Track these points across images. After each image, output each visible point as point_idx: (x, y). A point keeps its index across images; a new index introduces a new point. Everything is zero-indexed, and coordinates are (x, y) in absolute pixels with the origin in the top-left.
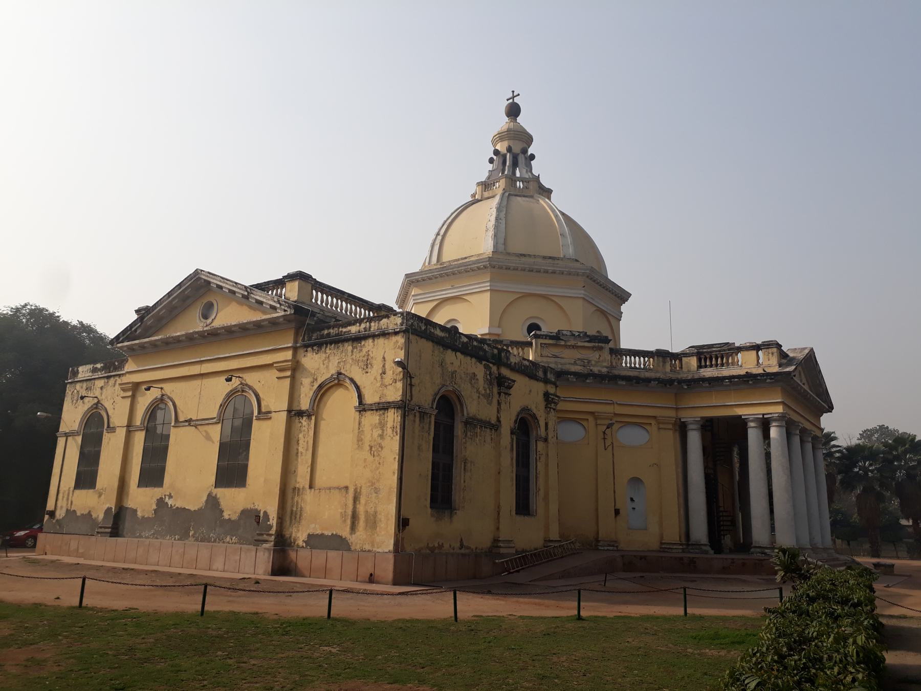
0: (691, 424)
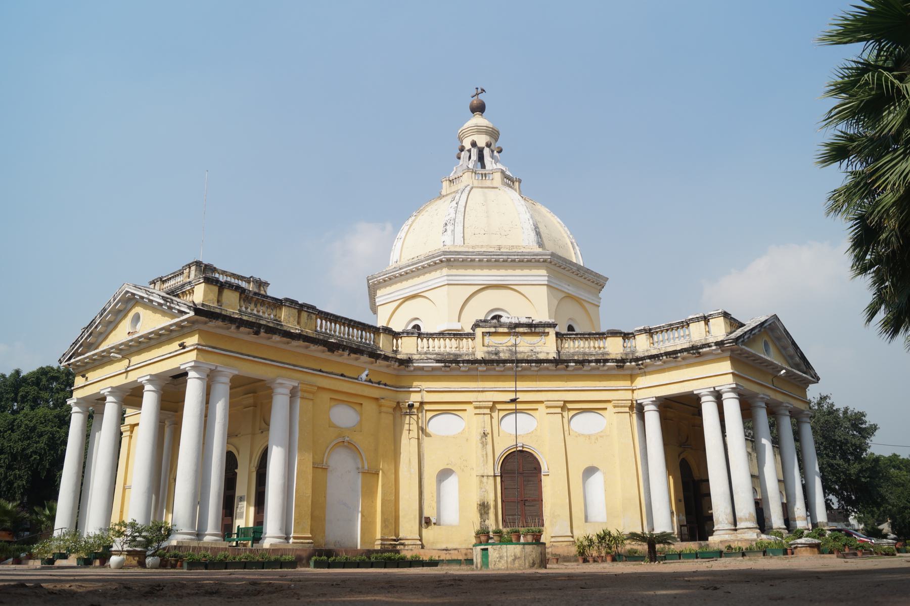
0: (647, 405)
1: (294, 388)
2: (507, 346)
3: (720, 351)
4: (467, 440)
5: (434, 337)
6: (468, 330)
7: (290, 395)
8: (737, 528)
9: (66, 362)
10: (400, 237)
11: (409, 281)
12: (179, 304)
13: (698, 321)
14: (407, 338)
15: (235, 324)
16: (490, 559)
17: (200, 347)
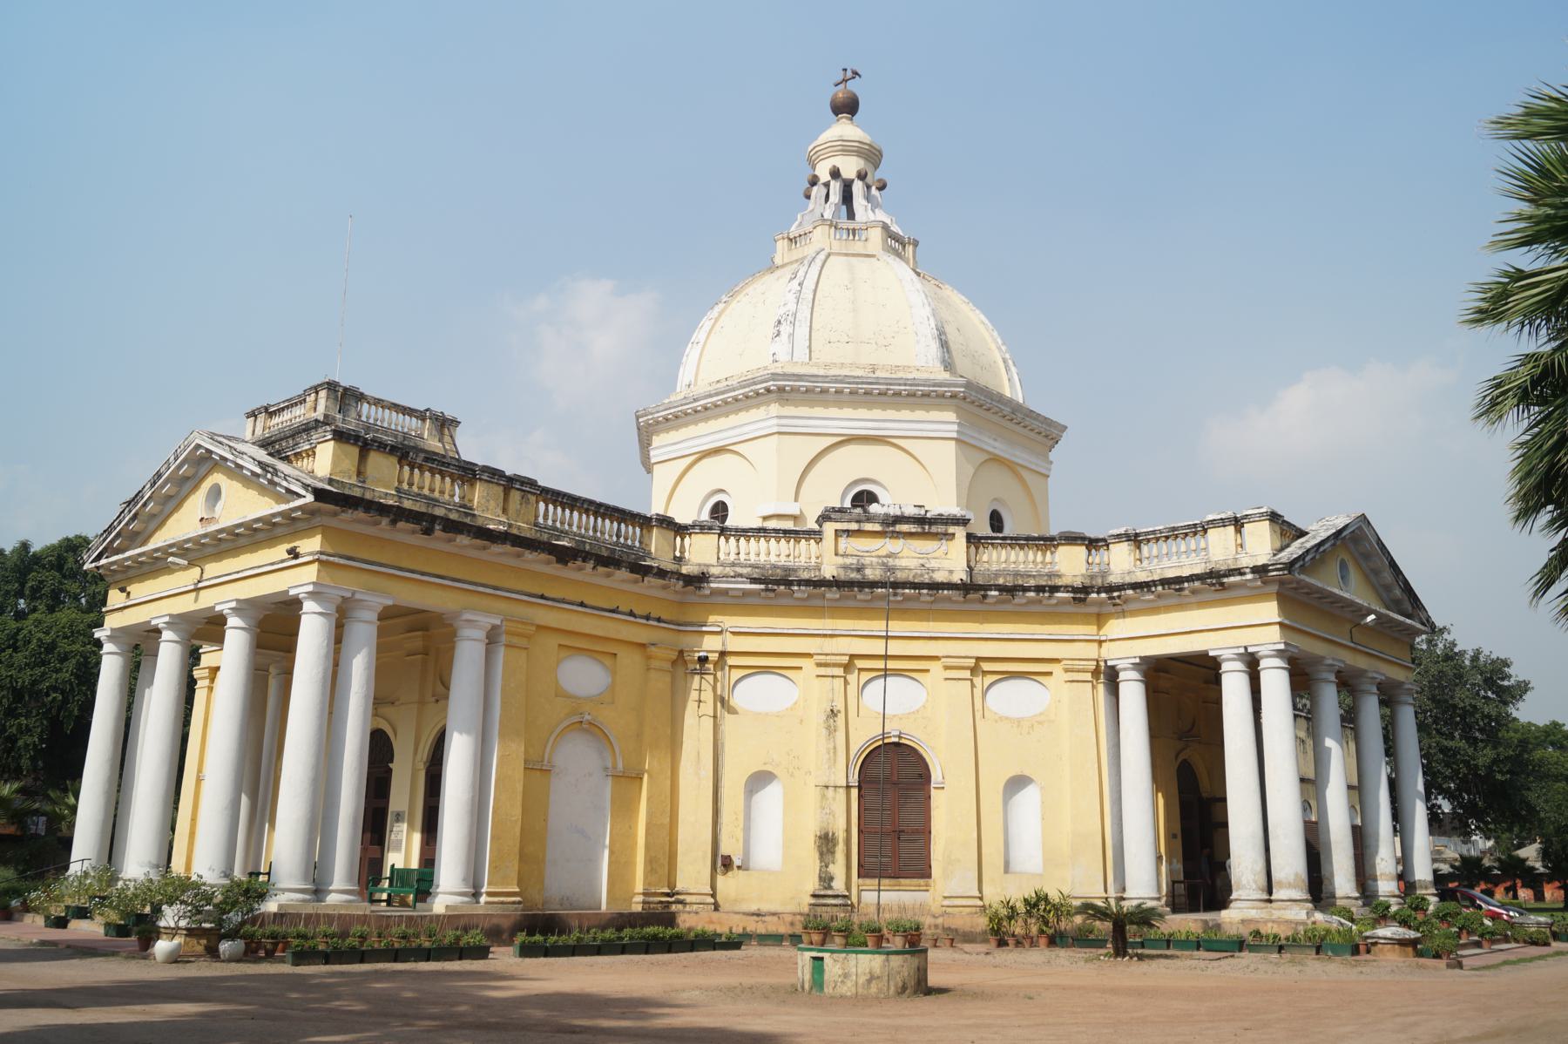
0: (1125, 669)
1: (494, 627)
2: (879, 557)
3: (1259, 583)
4: (802, 721)
5: (749, 536)
6: (812, 525)
7: (487, 641)
8: (1272, 898)
9: (92, 562)
10: (696, 341)
11: (710, 422)
12: (288, 478)
13: (1224, 526)
14: (700, 535)
15: (388, 516)
16: (826, 976)
17: (324, 557)
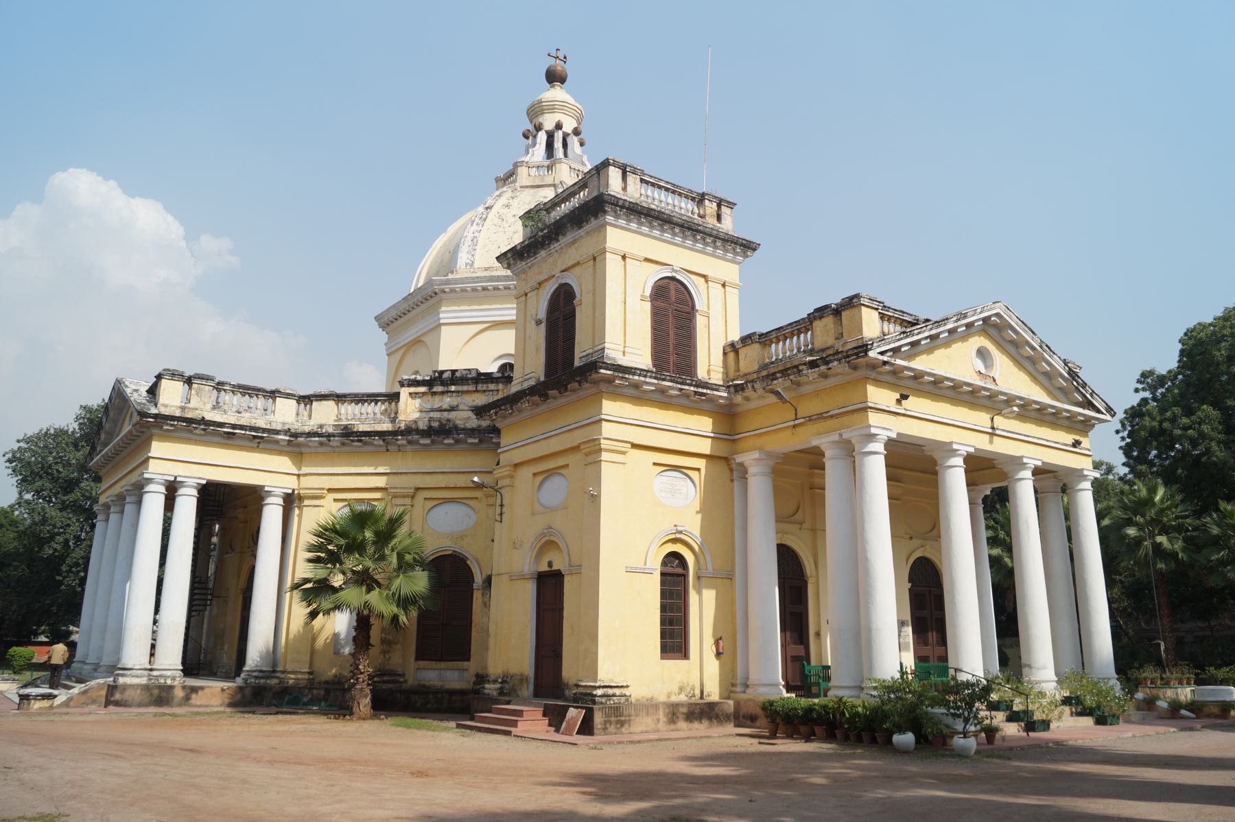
12: (1094, 394)
